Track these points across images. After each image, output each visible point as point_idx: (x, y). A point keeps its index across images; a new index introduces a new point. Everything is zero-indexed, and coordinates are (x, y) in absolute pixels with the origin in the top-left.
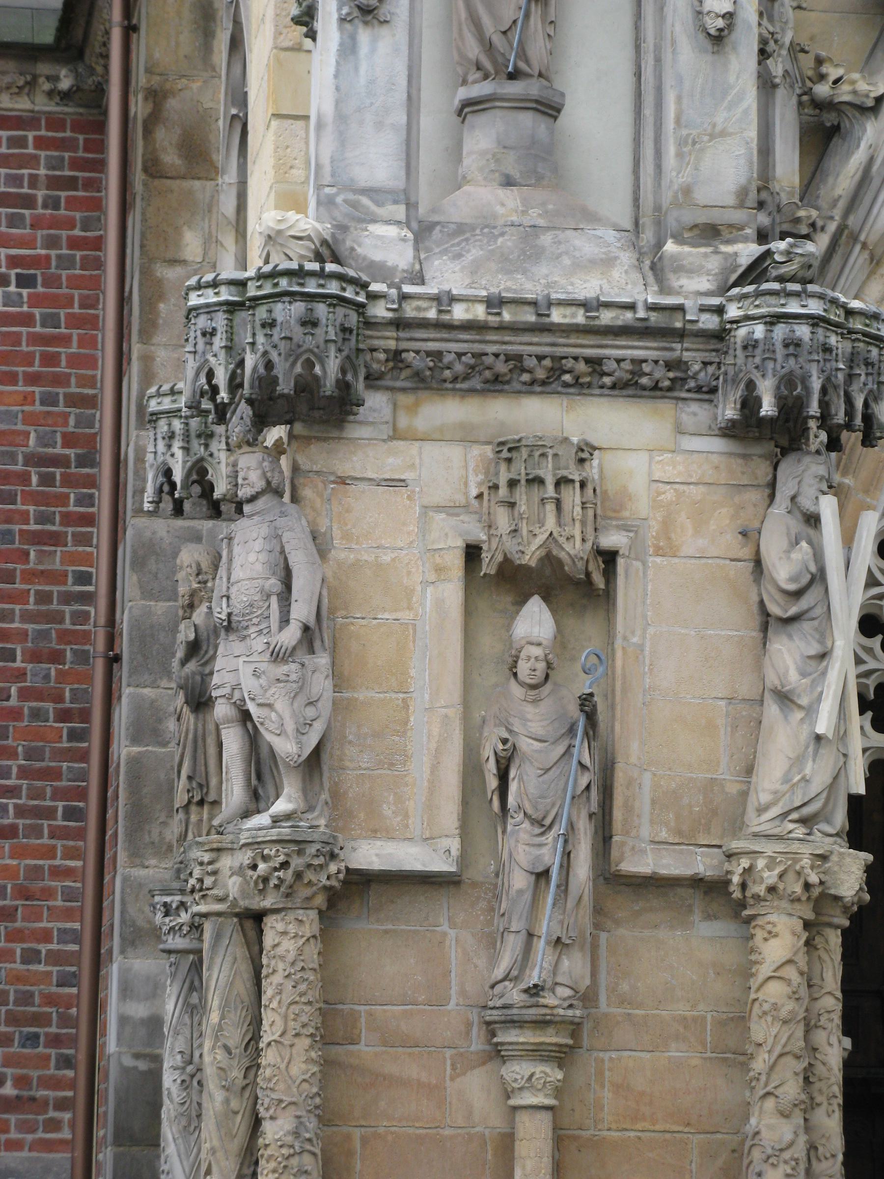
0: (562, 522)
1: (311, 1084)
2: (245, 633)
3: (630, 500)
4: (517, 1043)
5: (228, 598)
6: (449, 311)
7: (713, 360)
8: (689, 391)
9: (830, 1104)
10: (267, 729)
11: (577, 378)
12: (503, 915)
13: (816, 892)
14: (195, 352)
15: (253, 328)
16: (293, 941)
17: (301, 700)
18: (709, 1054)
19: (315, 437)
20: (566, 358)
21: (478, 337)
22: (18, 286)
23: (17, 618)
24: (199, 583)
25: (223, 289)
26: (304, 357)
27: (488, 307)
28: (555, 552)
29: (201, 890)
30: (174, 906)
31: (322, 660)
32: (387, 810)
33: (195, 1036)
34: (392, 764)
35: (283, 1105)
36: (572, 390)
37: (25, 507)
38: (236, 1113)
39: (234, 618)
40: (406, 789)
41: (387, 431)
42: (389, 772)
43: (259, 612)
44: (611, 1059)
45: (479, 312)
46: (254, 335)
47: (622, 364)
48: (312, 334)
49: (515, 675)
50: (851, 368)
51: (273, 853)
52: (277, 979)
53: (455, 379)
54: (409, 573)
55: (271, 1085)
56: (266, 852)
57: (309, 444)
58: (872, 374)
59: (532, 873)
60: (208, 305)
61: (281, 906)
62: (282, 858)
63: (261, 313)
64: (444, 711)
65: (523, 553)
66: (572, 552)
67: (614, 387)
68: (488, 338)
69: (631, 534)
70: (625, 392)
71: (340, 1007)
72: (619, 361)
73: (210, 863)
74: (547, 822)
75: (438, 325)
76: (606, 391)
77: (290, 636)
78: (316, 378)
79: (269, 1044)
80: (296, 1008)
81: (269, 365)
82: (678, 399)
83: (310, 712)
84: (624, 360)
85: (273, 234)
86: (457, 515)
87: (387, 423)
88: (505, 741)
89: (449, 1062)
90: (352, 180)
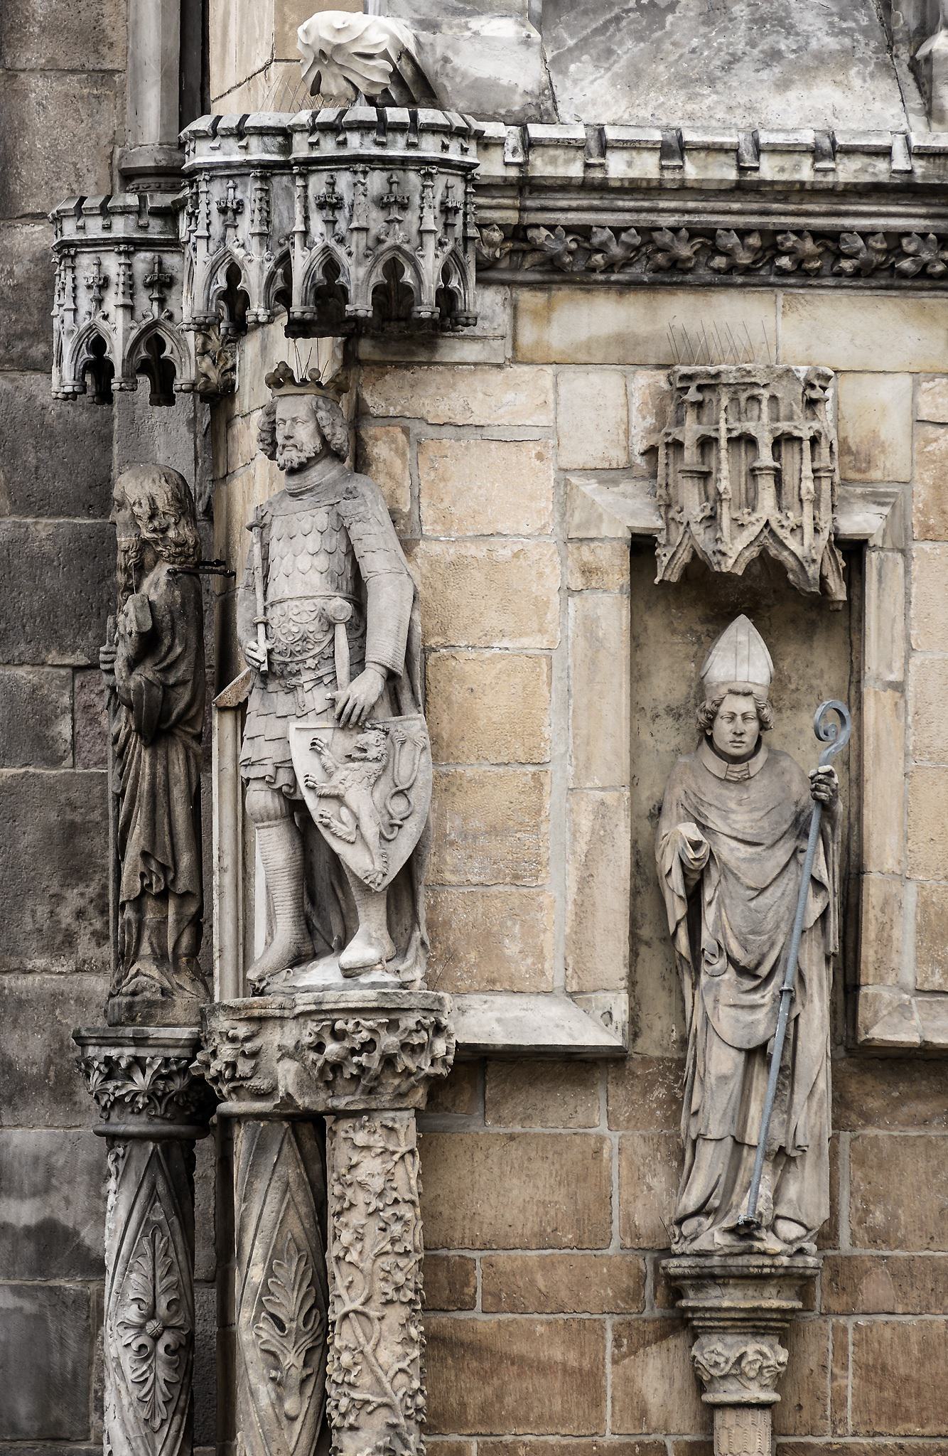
0: (784, 503)
1: (410, 1377)
2: (294, 681)
3: (883, 452)
4: (719, 1309)
5: (266, 624)
6: (602, 165)
10: (334, 834)
11: (799, 263)
12: (696, 1113)
14: (208, 238)
15: (306, 208)
16: (379, 1160)
17: (385, 787)
19: (391, 363)
21: (646, 204)
24: (155, 531)
25: (254, 142)
26: (388, 256)
27: (661, 158)
28: (773, 552)
29: (233, 1079)
30: (123, 1064)
31: (414, 724)
32: (512, 948)
33: (158, 1274)
34: (516, 877)
35: (370, 1408)
36: (792, 281)
38: (292, 1419)
39: (276, 657)
40: (539, 916)
42: (514, 889)
43: (317, 650)
44: (857, 1327)
45: (647, 167)
46: (306, 219)
47: (871, 242)
48: (400, 222)
49: (710, 740)
51: (350, 1027)
52: (356, 1218)
53: (610, 267)
54: (541, 575)
55: (351, 1378)
56: (339, 1025)
57: (383, 375)
59: (740, 1050)
60: (228, 165)
61: (361, 1106)
62: (365, 1035)
63: (317, 184)
64: (599, 795)
65: (724, 554)
66: (799, 551)
67: (857, 273)
68: (663, 204)
69: (886, 510)
70: (874, 283)
71: (443, 1252)
72: (865, 235)
73: (247, 1039)
74: (764, 970)
75: (586, 187)
76: (846, 282)
77: (368, 687)
78: (407, 290)
79: (346, 1316)
80: (385, 1263)
81: (332, 266)
83: (399, 806)
85: (328, 51)
86: (615, 482)
87: (503, 337)
88: (696, 845)
89: (609, 1336)
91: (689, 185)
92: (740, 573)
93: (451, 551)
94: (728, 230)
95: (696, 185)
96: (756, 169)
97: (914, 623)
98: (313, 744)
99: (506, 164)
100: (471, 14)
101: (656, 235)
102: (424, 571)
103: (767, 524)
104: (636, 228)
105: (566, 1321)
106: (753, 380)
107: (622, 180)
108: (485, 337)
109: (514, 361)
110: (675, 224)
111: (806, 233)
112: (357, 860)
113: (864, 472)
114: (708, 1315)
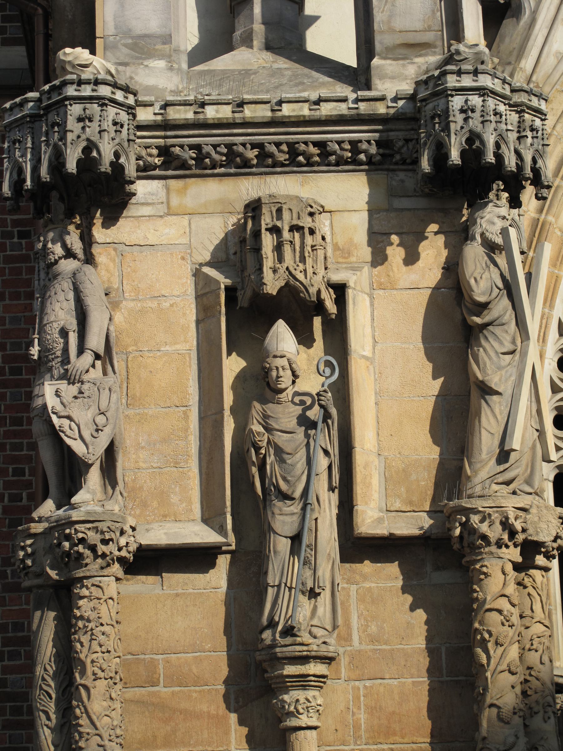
3: (356, 248)
7: (412, 137)
8: (396, 163)
9: (545, 712)
10: (66, 436)
13: (520, 537)
18: (445, 678)
20: (298, 143)
22: (18, 239)
23: (25, 448)
32: (174, 499)
34: (176, 463)
37: (28, 377)
40: (188, 482)
41: (162, 209)
42: (175, 469)
44: (365, 687)
47: (343, 145)
48: (89, 127)
50: (519, 132)
54: (184, 314)
58: (537, 137)
71: (142, 657)
72: (339, 143)
82: (388, 170)
83: (101, 420)
84: (343, 142)
87: (162, 203)
90: (130, 30)
91: (247, 120)
92: (275, 294)
93: (139, 305)
94: (270, 143)
95: (251, 120)
96: (280, 110)
97: (376, 329)
98: (57, 391)
99: (155, 114)
100: (145, 59)
101: (235, 147)
102: (125, 315)
103: (287, 269)
104: (224, 144)
105: (209, 690)
106: (278, 201)
107: (213, 119)
108: (153, 203)
109: (168, 214)
110: (243, 142)
111: (310, 143)
112: (78, 447)
113: (347, 258)
114: (278, 681)
